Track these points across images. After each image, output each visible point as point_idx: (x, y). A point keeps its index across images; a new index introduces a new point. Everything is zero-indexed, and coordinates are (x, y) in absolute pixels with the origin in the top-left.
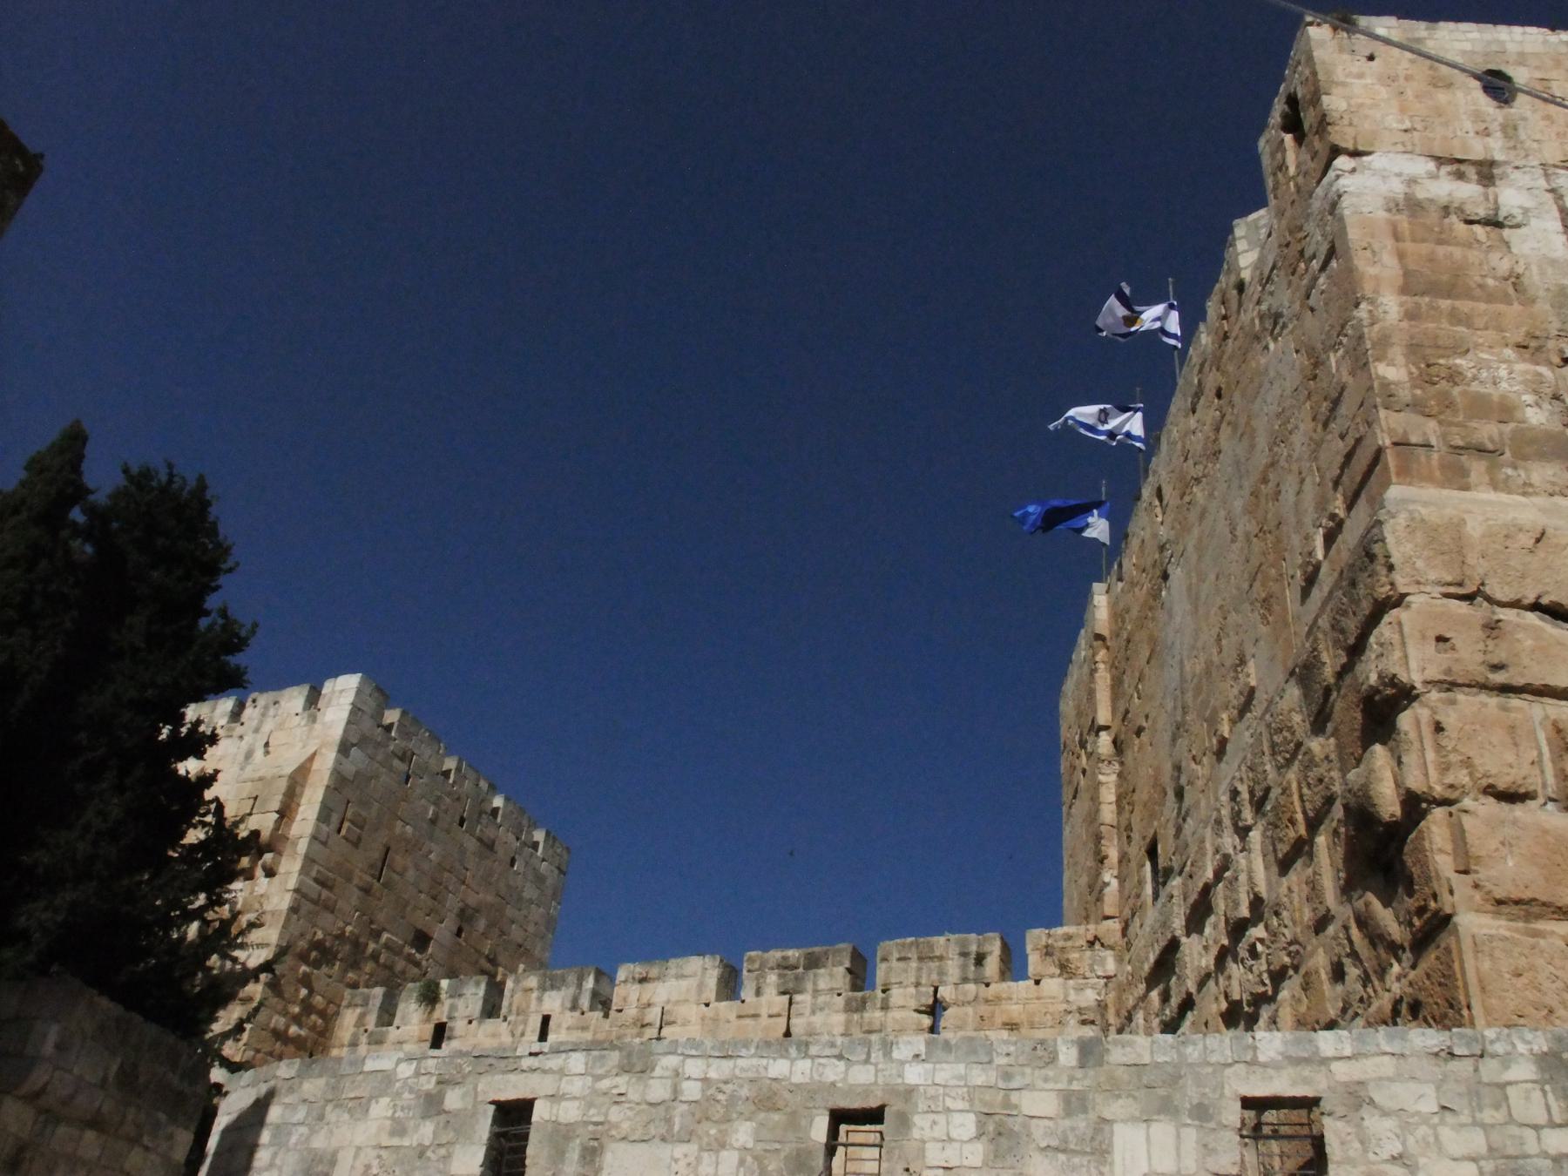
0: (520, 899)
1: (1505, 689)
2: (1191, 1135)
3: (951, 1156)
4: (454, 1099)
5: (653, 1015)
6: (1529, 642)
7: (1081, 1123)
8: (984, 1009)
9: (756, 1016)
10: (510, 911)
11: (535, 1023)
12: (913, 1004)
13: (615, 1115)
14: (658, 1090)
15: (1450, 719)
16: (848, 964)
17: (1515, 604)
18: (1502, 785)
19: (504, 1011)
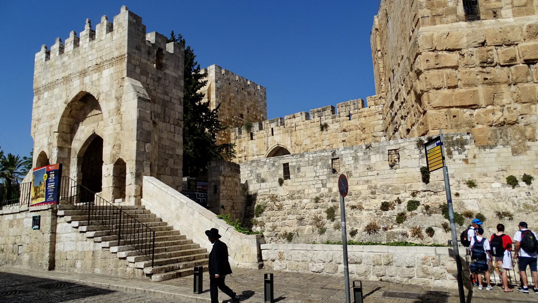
0: (258, 102)
1: (438, 68)
2: (381, 156)
3: (349, 163)
4: (276, 164)
5: (293, 125)
6: (443, 58)
7: (367, 156)
8: (359, 114)
9: (314, 122)
10: (257, 105)
11: (270, 130)
12: (345, 115)
13: (301, 163)
14: (306, 159)
15: (428, 77)
16: (331, 109)
17: (442, 50)
18: (436, 87)
19: (263, 128)
